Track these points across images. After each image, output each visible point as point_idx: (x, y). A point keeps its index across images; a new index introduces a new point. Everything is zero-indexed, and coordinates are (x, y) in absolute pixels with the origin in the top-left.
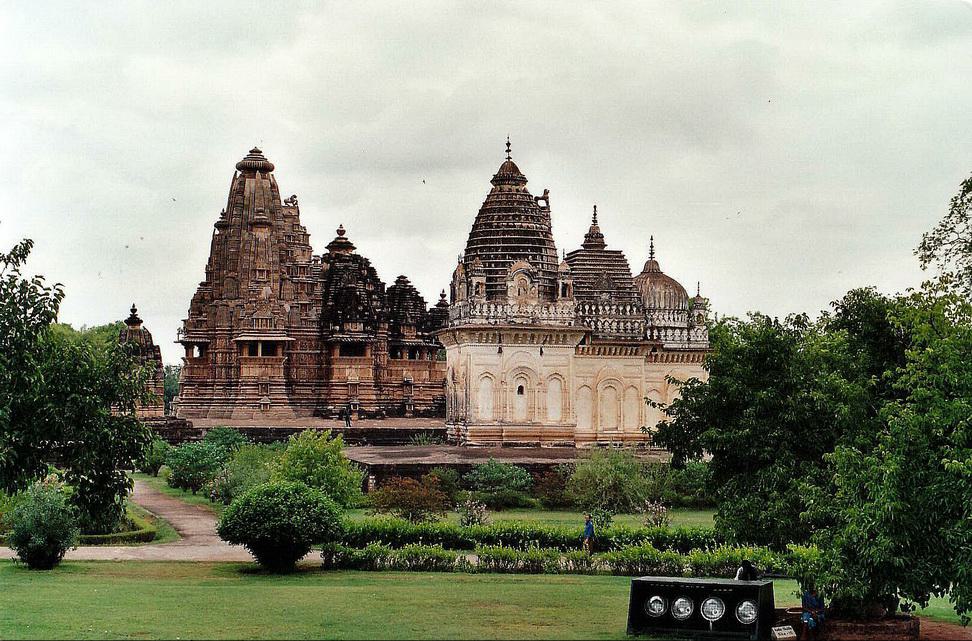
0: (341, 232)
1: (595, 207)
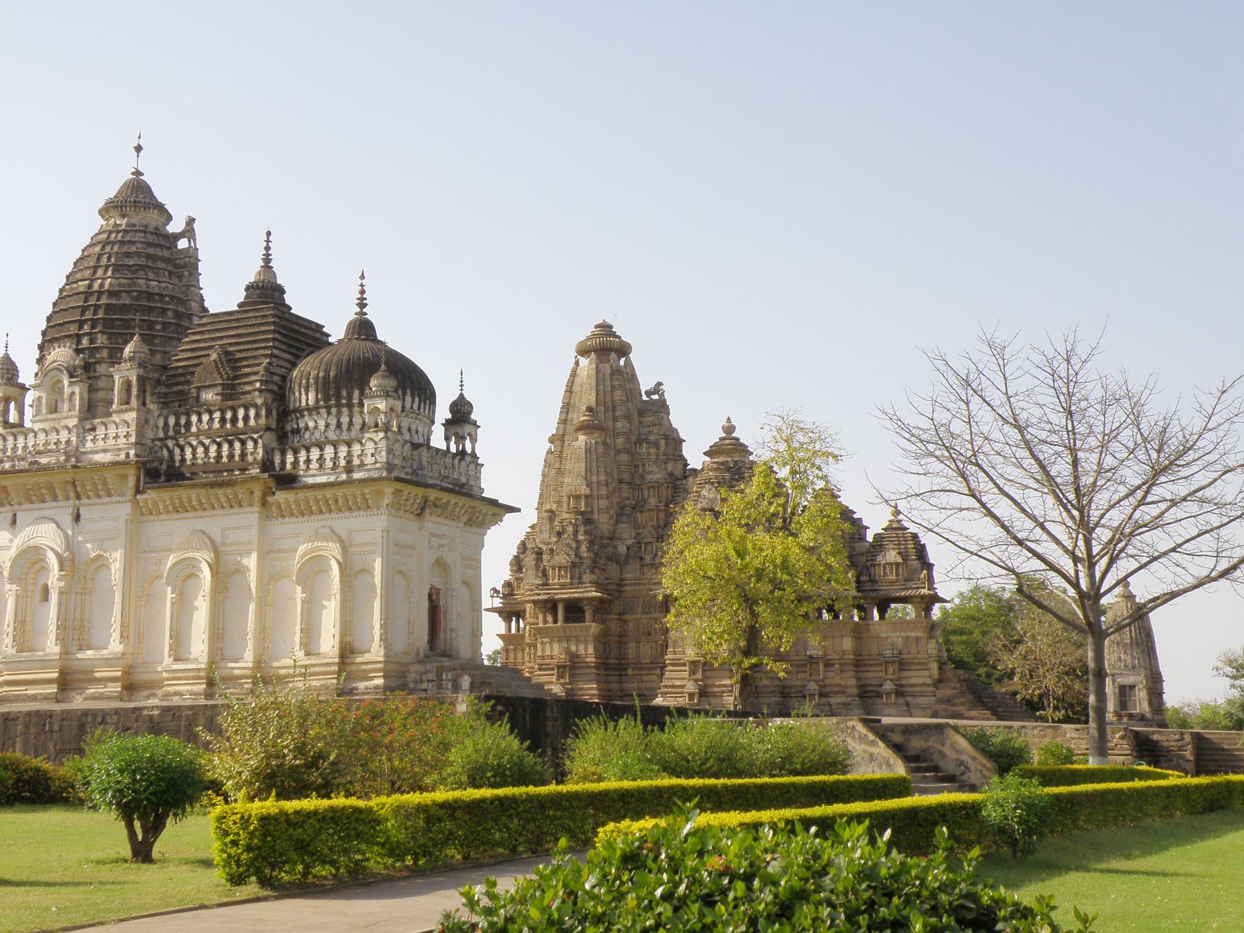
0: (729, 429)
1: (269, 234)
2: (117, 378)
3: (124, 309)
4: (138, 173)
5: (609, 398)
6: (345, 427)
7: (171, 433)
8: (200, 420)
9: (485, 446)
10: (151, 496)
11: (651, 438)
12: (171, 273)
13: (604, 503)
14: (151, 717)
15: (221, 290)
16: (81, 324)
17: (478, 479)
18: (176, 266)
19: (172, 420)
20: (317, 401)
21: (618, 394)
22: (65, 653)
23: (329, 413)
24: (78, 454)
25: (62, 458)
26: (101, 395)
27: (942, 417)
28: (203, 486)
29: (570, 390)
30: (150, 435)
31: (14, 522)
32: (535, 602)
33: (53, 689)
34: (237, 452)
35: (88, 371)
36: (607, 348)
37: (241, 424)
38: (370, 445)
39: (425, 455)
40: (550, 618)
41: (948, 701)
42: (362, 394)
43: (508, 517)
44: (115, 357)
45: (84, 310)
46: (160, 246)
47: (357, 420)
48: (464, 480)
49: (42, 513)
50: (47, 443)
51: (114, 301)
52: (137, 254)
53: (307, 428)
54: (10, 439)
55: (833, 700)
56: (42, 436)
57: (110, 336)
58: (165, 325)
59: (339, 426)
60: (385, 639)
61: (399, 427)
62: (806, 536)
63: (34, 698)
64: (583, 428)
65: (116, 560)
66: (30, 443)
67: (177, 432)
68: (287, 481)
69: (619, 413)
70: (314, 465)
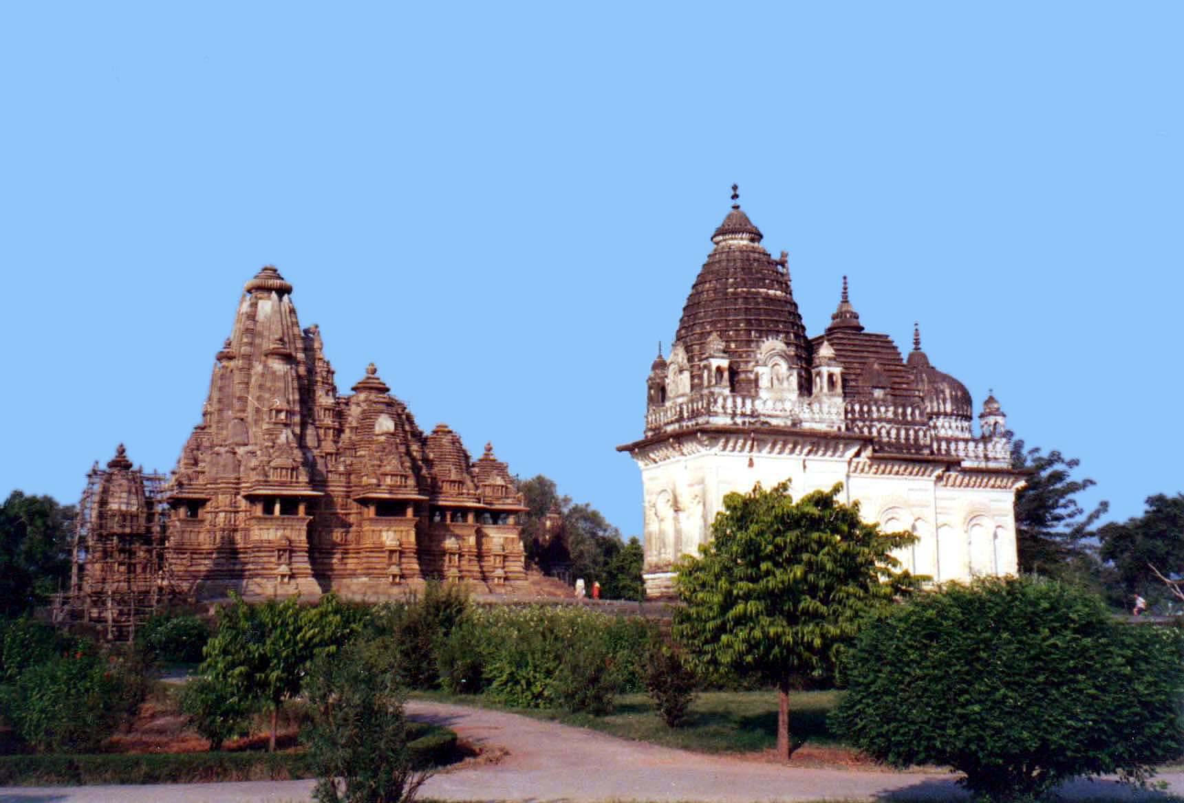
8: (878, 410)
19: (857, 407)
25: (789, 423)
34: (912, 437)
37: (909, 418)
53: (943, 427)
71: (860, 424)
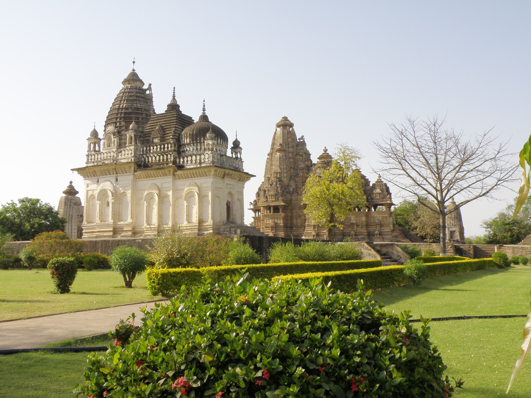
0: (326, 150)
1: (174, 88)
2: (128, 135)
3: (130, 113)
4: (134, 70)
5: (287, 141)
6: (199, 150)
7: (145, 153)
8: (153, 148)
9: (244, 155)
10: (139, 173)
11: (300, 154)
12: (144, 102)
13: (285, 175)
14: (139, 242)
15: (160, 106)
16: (117, 118)
17: (242, 166)
18: (146, 99)
19: (145, 149)
20: (190, 141)
21: (289, 139)
22: (115, 222)
23: (194, 145)
24: (117, 160)
26: (123, 141)
27: (393, 144)
28: (155, 169)
29: (274, 139)
30: (138, 153)
31: (98, 182)
32: (263, 207)
33: (111, 234)
34: (165, 158)
35: (119, 133)
36: (286, 125)
37: (166, 149)
38: (207, 155)
39: (224, 158)
40: (268, 212)
41: (396, 237)
42: (204, 139)
43: (252, 178)
44: (127, 129)
45: (117, 114)
46: (141, 93)
47: (203, 147)
48: (237, 166)
49: (106, 179)
50: (107, 157)
51: (126, 111)
52: (134, 96)
53: (187, 150)
54: (96, 155)
55: (359, 237)
56: (105, 154)
57: (126, 122)
58: (143, 118)
59: (197, 149)
60: (213, 218)
61: (216, 150)
62: (349, 184)
63: (106, 236)
64: (278, 150)
65: (129, 193)
66: (102, 157)
67: (147, 152)
68: (181, 167)
69: (290, 146)
70: (189, 162)
71: (144, 156)
